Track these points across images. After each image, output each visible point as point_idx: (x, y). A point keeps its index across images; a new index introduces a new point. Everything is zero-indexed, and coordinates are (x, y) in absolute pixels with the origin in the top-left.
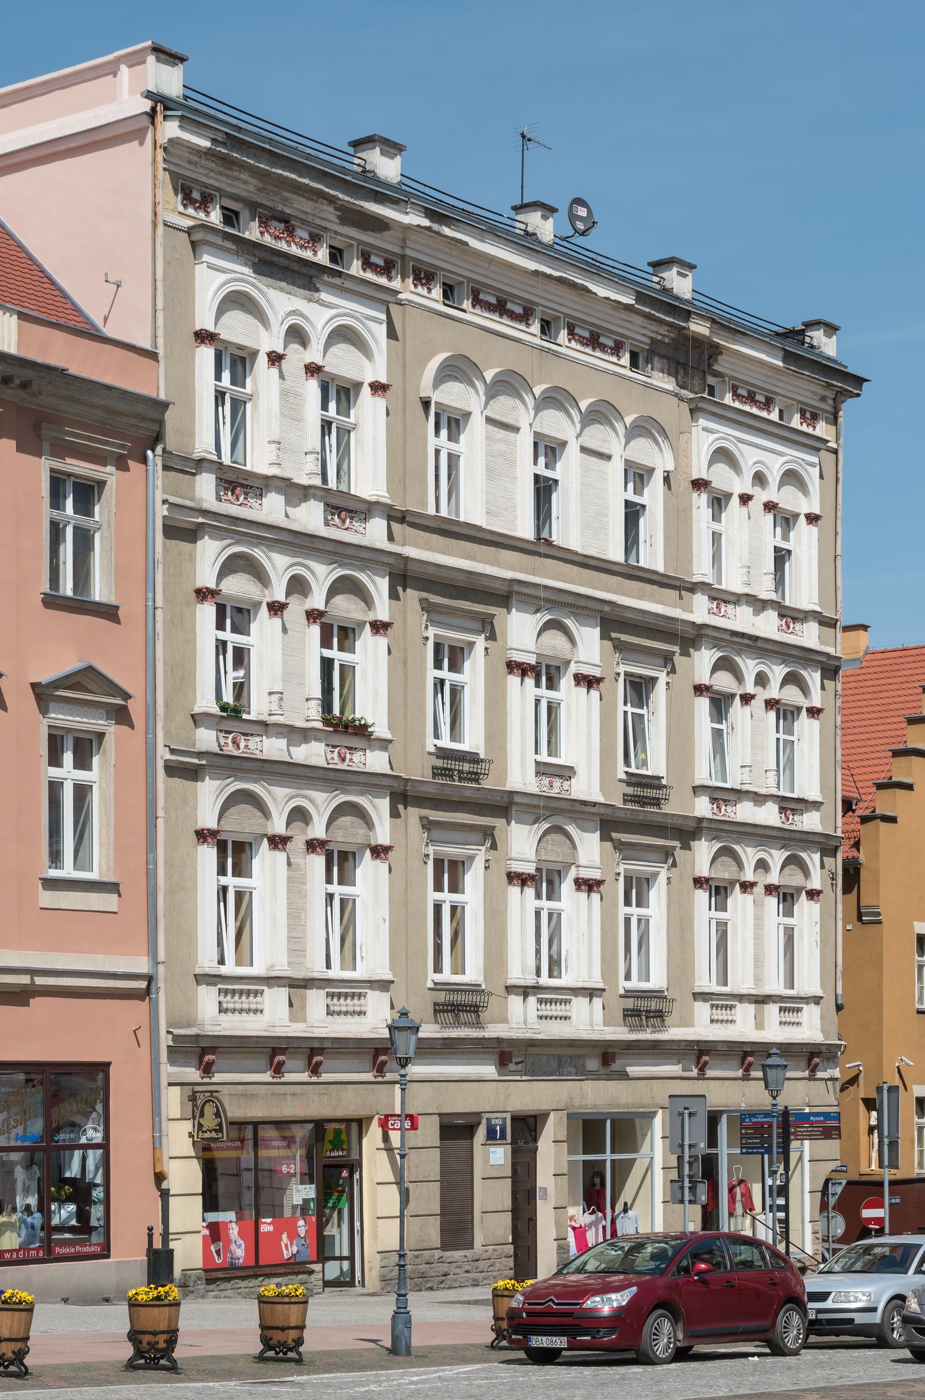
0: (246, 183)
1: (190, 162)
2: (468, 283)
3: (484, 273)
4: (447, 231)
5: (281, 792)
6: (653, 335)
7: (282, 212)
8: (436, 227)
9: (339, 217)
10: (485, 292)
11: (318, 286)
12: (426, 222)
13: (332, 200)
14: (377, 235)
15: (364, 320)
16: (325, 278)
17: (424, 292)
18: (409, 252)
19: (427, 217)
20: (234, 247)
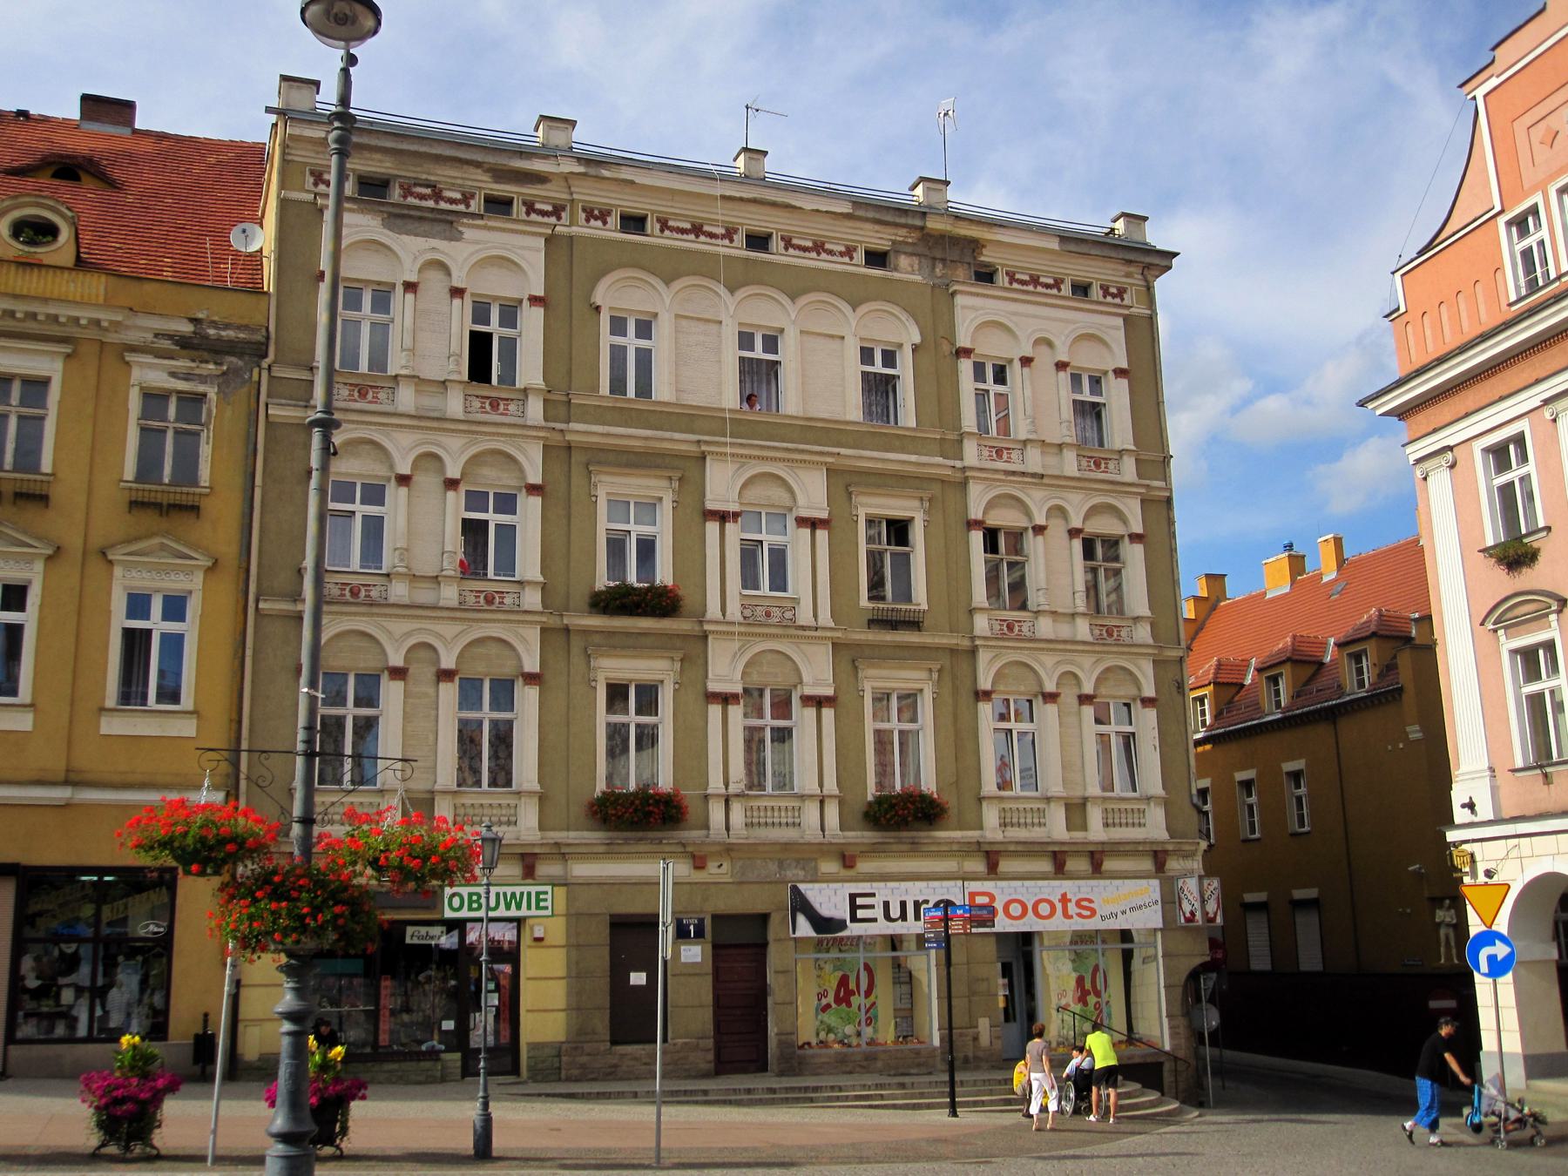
0: (380, 161)
1: (318, 153)
2: (652, 215)
3: (669, 204)
4: (606, 173)
6: (893, 238)
7: (427, 180)
8: (592, 171)
9: (493, 177)
10: (675, 220)
11: (460, 229)
12: (581, 169)
13: (478, 165)
14: (539, 186)
15: (519, 251)
16: (465, 220)
17: (599, 223)
18: (575, 196)
19: (580, 165)
20: (355, 207)
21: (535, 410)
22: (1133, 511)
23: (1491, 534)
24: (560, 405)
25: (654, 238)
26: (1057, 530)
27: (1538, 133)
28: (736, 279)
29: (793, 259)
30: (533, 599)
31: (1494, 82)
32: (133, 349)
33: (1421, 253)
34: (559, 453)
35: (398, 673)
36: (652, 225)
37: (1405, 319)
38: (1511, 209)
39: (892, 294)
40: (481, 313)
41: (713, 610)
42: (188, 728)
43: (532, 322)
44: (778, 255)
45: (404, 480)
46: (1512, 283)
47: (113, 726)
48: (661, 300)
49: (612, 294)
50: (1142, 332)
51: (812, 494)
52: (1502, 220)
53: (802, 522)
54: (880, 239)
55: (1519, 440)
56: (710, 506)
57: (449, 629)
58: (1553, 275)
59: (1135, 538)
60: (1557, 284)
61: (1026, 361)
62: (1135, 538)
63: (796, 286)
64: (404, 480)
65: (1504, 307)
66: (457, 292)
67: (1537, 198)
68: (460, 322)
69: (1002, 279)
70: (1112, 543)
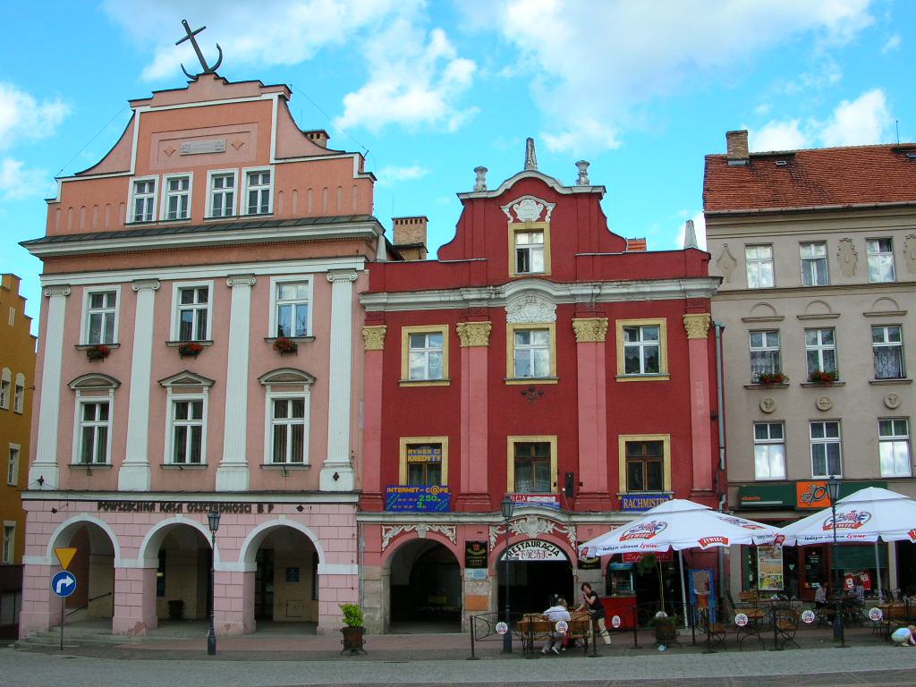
23: (84, 340)
27: (165, 145)
31: (148, 109)
33: (78, 175)
37: (58, 206)
38: (140, 176)
46: (130, 216)
52: (132, 180)
55: (112, 295)
58: (154, 219)
60: (155, 224)
65: (121, 224)
67: (156, 178)
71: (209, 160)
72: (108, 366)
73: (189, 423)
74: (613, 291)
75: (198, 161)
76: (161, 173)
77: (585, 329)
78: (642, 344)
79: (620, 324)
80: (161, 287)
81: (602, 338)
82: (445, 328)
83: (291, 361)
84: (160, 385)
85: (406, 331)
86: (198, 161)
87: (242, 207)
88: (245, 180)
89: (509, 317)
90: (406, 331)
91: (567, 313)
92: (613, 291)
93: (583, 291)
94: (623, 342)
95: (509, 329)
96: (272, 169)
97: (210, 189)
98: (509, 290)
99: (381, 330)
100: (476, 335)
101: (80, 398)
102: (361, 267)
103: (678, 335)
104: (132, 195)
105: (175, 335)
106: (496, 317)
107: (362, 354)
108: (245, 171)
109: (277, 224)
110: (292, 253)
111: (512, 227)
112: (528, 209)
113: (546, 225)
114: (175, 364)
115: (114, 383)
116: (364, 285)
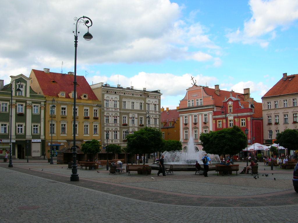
5: (111, 127)
21: (119, 110)
22: (158, 116)
24: (120, 109)
25: (126, 95)
26: (153, 118)
28: (131, 98)
29: (136, 96)
30: (119, 125)
32: (93, 107)
34: (120, 113)
35: (110, 131)
36: (126, 94)
39: (142, 99)
40: (114, 102)
41: (130, 126)
42: (98, 135)
43: (118, 103)
44: (134, 96)
45: (110, 116)
47: (94, 135)
48: (126, 100)
49: (124, 100)
50: (159, 100)
51: (136, 116)
53: (136, 118)
54: (141, 94)
56: (130, 117)
57: (114, 128)
59: (158, 118)
61: (151, 104)
62: (158, 118)
63: (135, 98)
64: (110, 116)
66: (113, 100)
68: (113, 103)
69: (149, 97)
70: (156, 119)
71: (195, 98)
72: (187, 126)
73: (196, 133)
74: (239, 114)
75: (194, 98)
76: (191, 99)
77: (236, 120)
78: (243, 121)
79: (240, 119)
80: (192, 115)
81: (238, 121)
82: (221, 120)
83: (206, 125)
84: (193, 128)
85: (218, 121)
86: (194, 98)
87: (199, 104)
88: (200, 100)
89: (228, 119)
90: (218, 121)
91: (235, 117)
92: (239, 114)
93: (236, 115)
94: (241, 122)
95: (228, 120)
96: (202, 98)
97: (196, 101)
98: (228, 115)
99: (215, 121)
100: (224, 121)
101: (185, 130)
102: (212, 112)
103: (247, 120)
104: (188, 103)
105: (194, 122)
106: (226, 118)
107: (213, 124)
108: (200, 99)
109: (202, 107)
110: (205, 110)
111: (228, 106)
112: (230, 103)
113: (232, 105)
114: (194, 126)
115: (188, 128)
116: (213, 115)
